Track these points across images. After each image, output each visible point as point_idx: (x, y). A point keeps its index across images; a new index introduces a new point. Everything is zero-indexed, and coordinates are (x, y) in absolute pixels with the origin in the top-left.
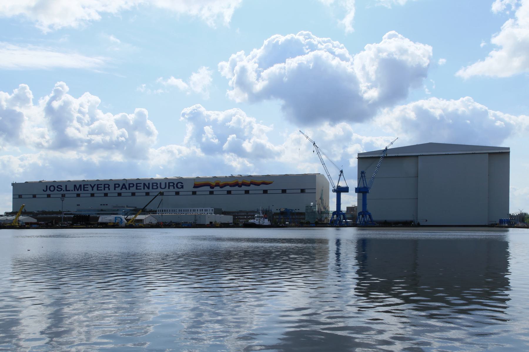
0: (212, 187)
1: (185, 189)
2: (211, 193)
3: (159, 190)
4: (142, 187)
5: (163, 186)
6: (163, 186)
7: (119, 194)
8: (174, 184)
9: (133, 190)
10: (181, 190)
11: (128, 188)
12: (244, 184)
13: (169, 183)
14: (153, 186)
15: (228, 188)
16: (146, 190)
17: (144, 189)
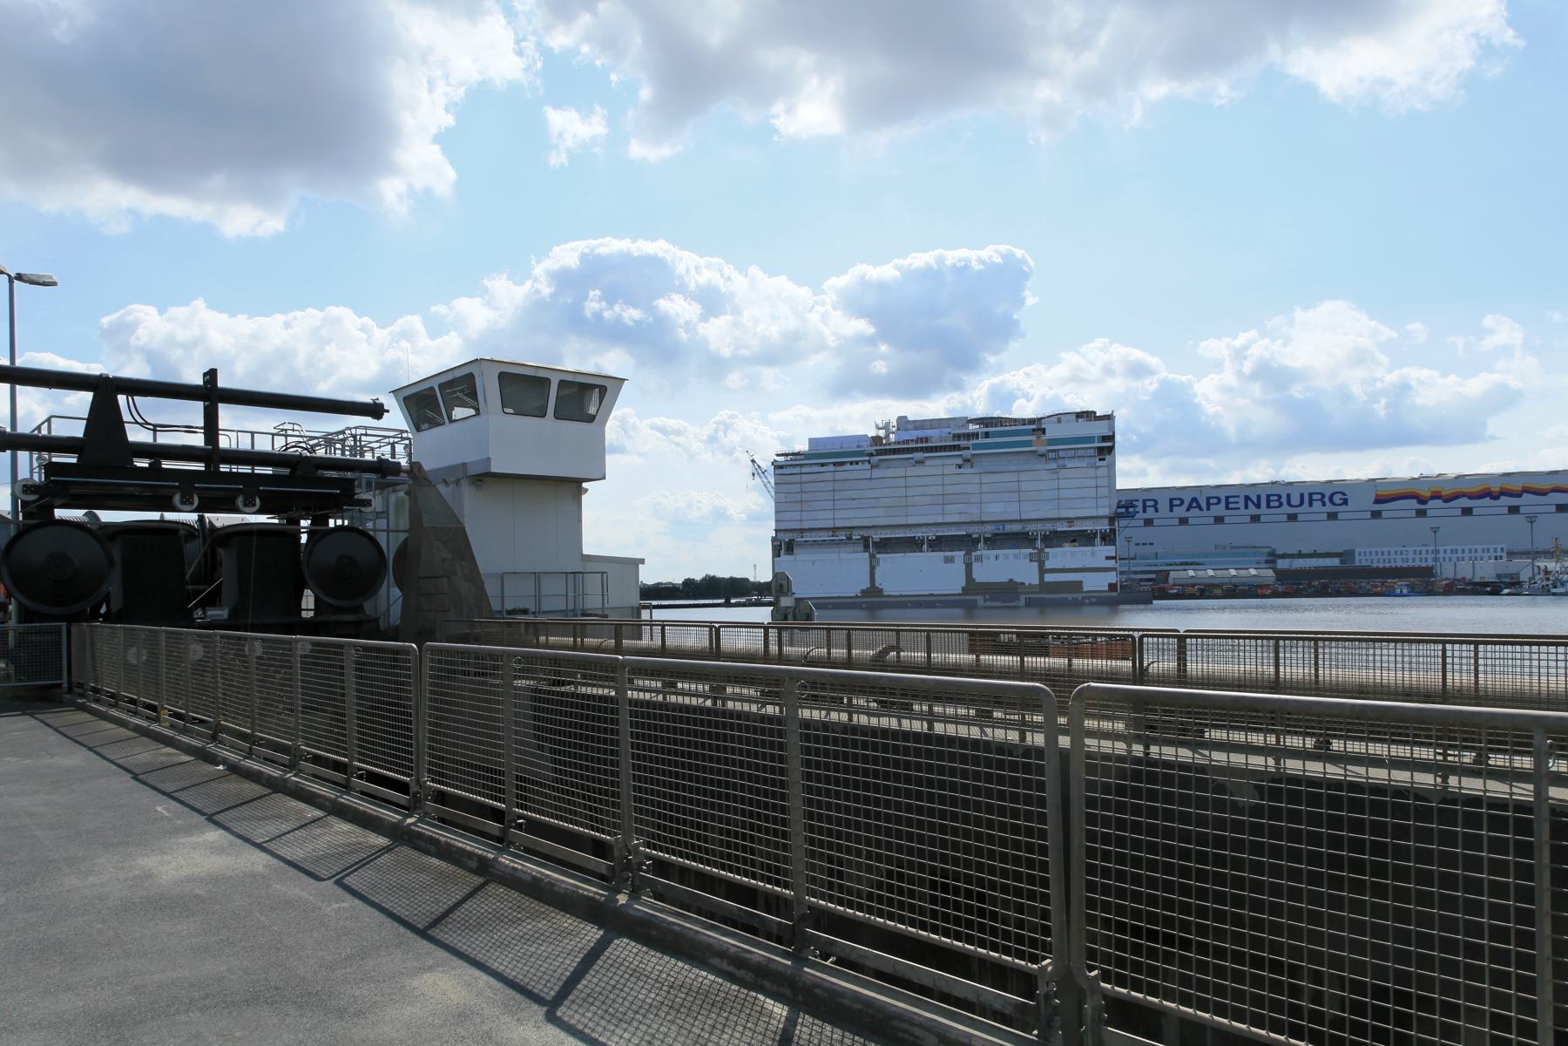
0: (1422, 501)
1: (1352, 505)
2: (1421, 513)
3: (1286, 509)
4: (1242, 505)
5: (1296, 501)
6: (1296, 501)
7: (1183, 521)
8: (1323, 496)
9: (1219, 510)
10: (1343, 508)
11: (1204, 505)
12: (1505, 493)
13: (1311, 495)
14: (1268, 501)
15: (1465, 502)
16: (1252, 510)
17: (1246, 507)
